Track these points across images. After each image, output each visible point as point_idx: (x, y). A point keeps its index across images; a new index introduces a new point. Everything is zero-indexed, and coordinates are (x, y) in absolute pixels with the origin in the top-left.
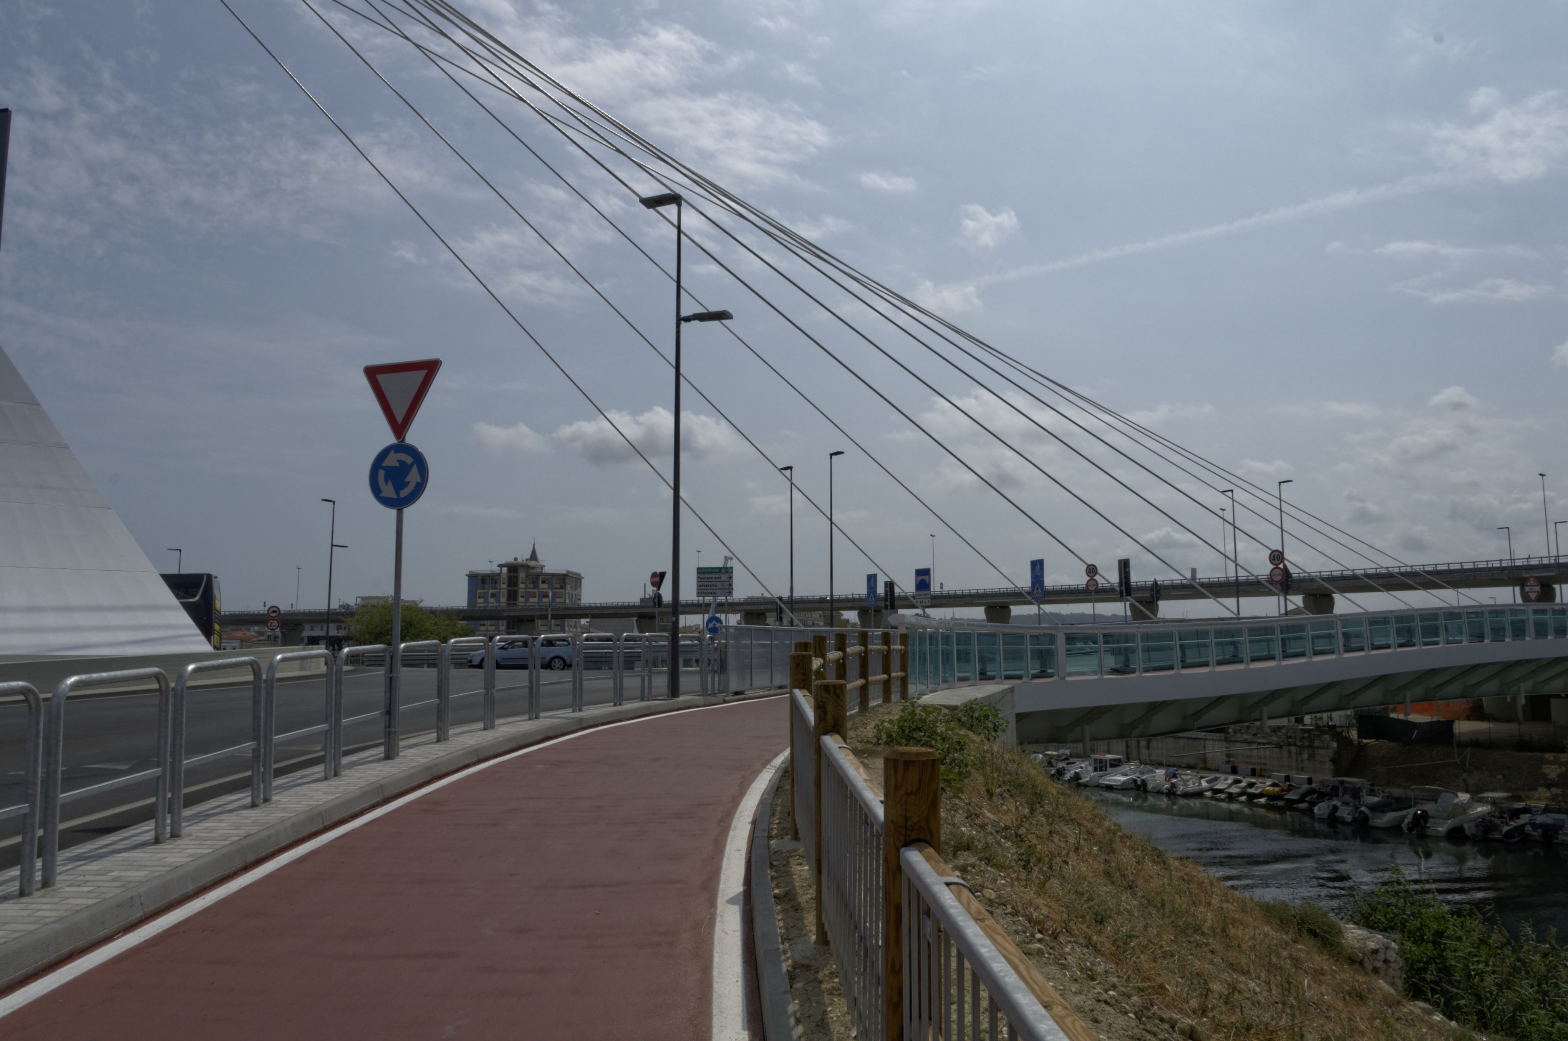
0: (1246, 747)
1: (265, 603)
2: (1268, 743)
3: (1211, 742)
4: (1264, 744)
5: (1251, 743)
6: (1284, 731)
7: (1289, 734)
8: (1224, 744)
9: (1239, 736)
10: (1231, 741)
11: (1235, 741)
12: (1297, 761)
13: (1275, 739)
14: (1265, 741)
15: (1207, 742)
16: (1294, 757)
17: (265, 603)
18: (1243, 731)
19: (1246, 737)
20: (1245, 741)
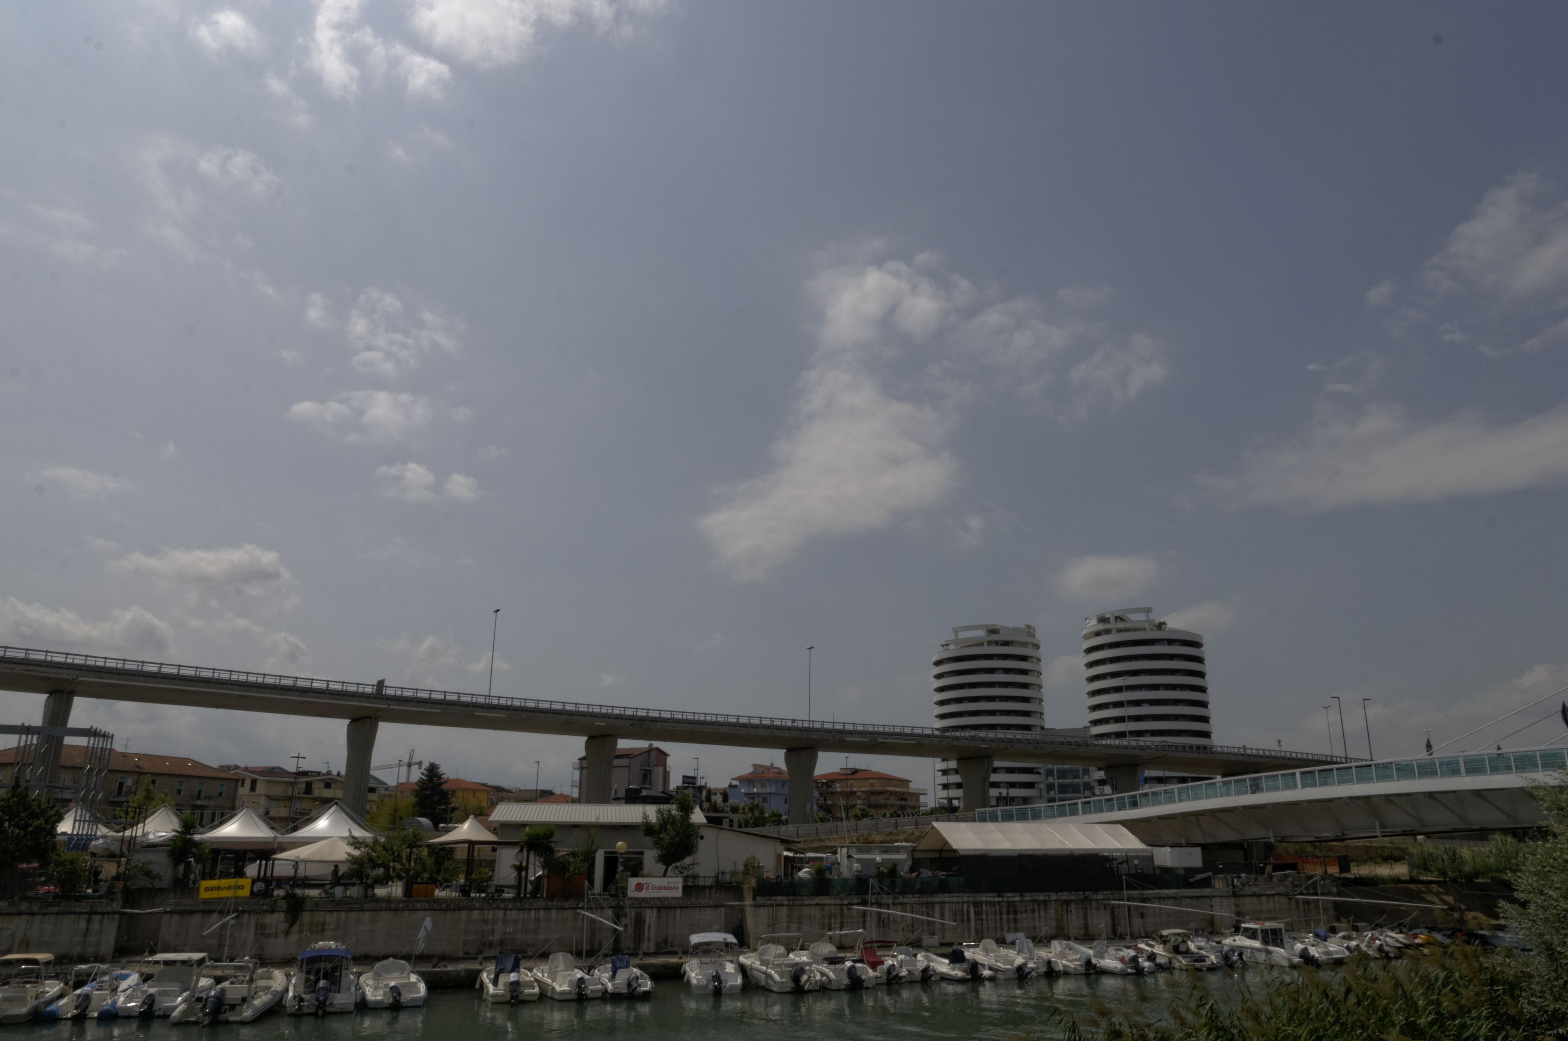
0: (1254, 899)
2: (1277, 894)
3: (1218, 900)
4: (1272, 895)
6: (1290, 879)
7: (1296, 883)
8: (1233, 900)
9: (1247, 890)
12: (1304, 911)
13: (1282, 889)
15: (1214, 900)
16: (1301, 906)
18: (1251, 883)
19: (1255, 889)
20: (1254, 895)
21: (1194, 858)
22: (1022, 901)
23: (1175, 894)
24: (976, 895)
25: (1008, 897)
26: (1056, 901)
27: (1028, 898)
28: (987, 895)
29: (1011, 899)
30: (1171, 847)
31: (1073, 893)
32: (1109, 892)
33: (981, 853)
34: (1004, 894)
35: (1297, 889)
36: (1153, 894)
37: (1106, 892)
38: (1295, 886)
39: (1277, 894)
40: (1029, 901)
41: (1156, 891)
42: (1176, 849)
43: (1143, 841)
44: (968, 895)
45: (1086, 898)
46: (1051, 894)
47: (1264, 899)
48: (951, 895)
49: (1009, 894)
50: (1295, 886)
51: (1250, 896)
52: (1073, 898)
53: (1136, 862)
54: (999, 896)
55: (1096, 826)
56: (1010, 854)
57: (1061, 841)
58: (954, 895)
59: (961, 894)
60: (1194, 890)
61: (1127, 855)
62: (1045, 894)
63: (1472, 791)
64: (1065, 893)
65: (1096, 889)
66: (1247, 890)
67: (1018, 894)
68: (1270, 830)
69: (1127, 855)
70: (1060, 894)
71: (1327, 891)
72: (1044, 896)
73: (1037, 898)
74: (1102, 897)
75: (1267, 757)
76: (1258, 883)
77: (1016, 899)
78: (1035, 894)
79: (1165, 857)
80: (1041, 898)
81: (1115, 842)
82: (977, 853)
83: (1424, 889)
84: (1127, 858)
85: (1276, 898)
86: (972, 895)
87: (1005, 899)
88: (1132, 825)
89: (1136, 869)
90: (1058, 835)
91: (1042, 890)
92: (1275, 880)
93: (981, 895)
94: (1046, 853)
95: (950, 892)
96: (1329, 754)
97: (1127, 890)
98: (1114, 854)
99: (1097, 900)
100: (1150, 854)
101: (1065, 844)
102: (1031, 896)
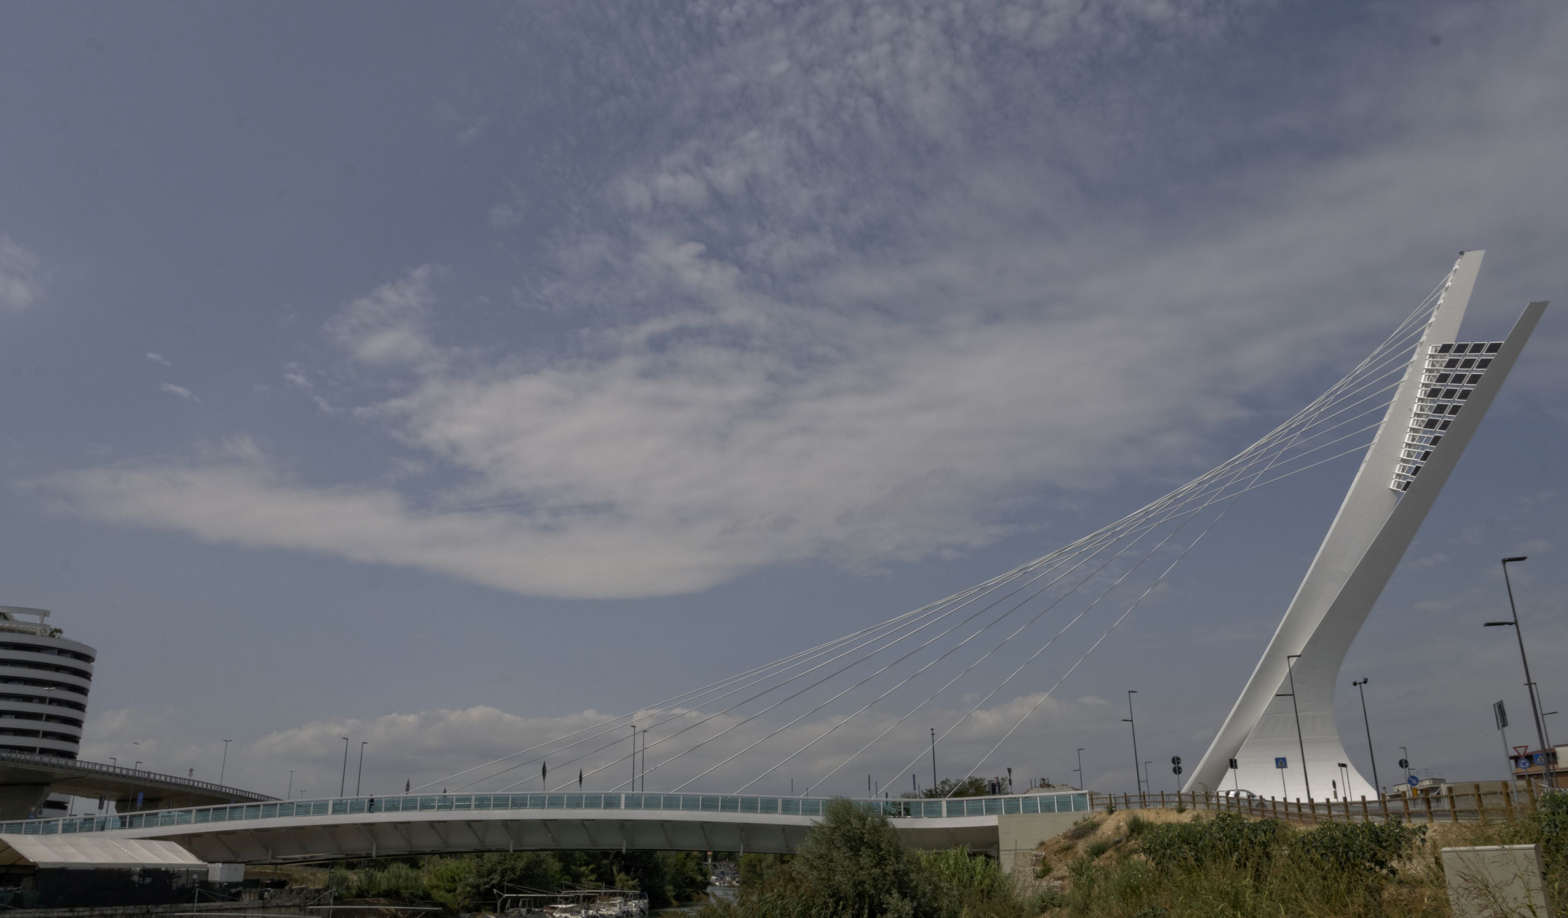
1: (1176, 760)
2: (294, 906)
4: (290, 906)
5: (281, 907)
6: (304, 892)
7: (308, 895)
9: (274, 902)
10: (267, 908)
11: (270, 908)
13: (297, 901)
14: (291, 904)
17: (1176, 760)
18: (277, 896)
19: (279, 902)
21: (236, 873)
22: (91, 916)
23: (220, 906)
24: (48, 910)
25: (79, 912)
26: (122, 914)
27: (97, 913)
28: (60, 910)
29: (81, 914)
30: (224, 863)
31: (138, 907)
32: (168, 906)
33: (61, 866)
34: (75, 909)
35: (307, 901)
36: (203, 907)
37: (165, 906)
38: (307, 898)
39: (294, 906)
40: (98, 915)
41: (206, 904)
42: (226, 865)
43: (199, 856)
44: (40, 910)
45: (148, 911)
46: (118, 908)
47: (283, 910)
48: (24, 910)
49: (80, 909)
50: (307, 898)
51: (274, 907)
52: (137, 911)
53: (195, 876)
54: (70, 911)
55: (132, 841)
56: (88, 868)
57: (130, 856)
58: (27, 911)
59: (34, 910)
60: (235, 902)
61: (188, 871)
62: (114, 908)
63: (428, 822)
64: (131, 907)
65: (157, 903)
66: (274, 902)
67: (88, 909)
68: (270, 852)
69: (188, 871)
70: (126, 908)
71: (326, 902)
72: (112, 910)
73: (105, 912)
74: (162, 911)
75: (168, 783)
76: (282, 895)
77: (87, 913)
78: (104, 908)
79: (218, 873)
80: (109, 912)
81: (176, 858)
82: (52, 867)
83: (376, 902)
84: (189, 871)
85: (292, 909)
86: (44, 910)
87: (75, 914)
88: (187, 841)
89: (194, 883)
90: (126, 851)
91: (110, 905)
92: (294, 893)
93: (54, 910)
94: (120, 867)
95: (22, 908)
96: (218, 783)
97: (199, 902)
98: (181, 869)
99: (157, 913)
100: (205, 869)
101: (136, 859)
102: (100, 911)
